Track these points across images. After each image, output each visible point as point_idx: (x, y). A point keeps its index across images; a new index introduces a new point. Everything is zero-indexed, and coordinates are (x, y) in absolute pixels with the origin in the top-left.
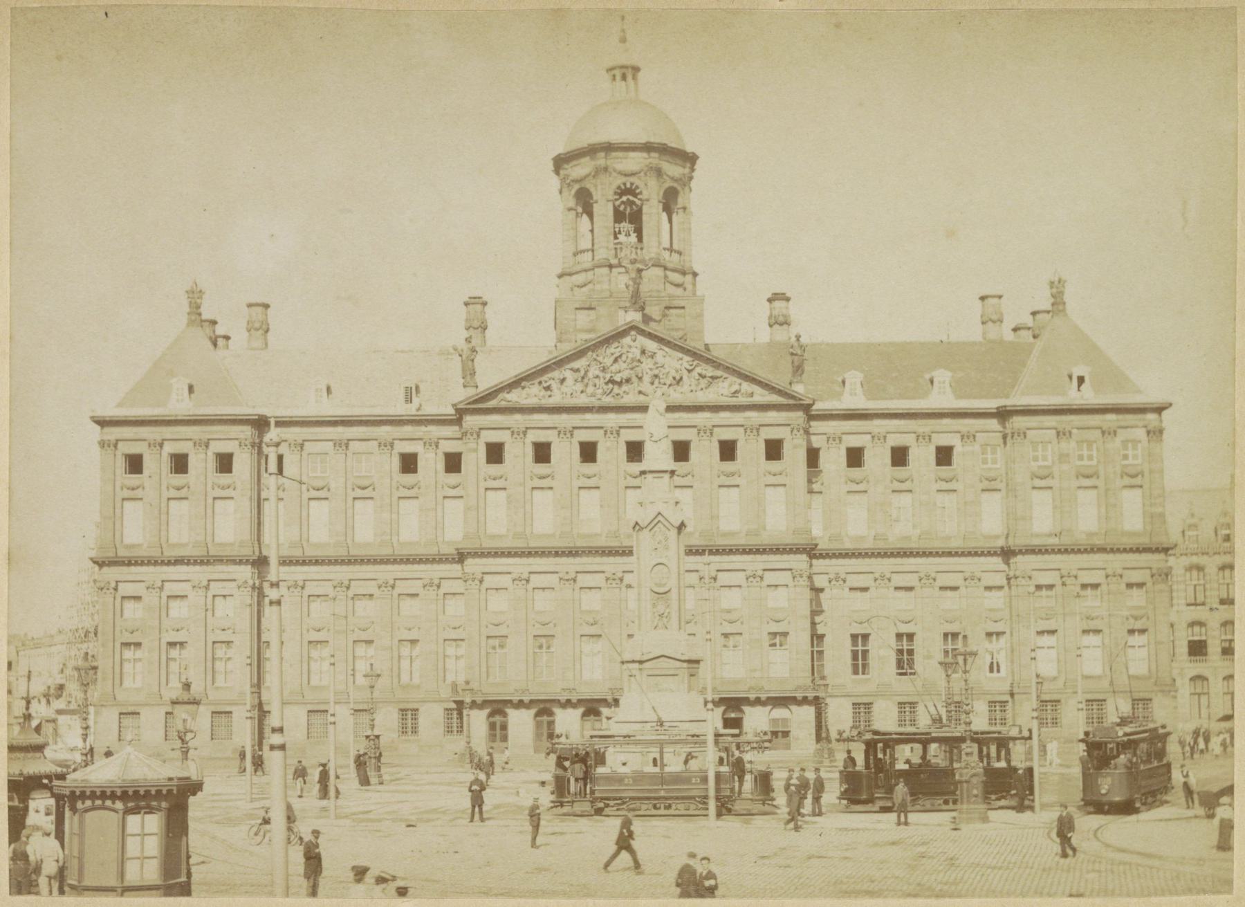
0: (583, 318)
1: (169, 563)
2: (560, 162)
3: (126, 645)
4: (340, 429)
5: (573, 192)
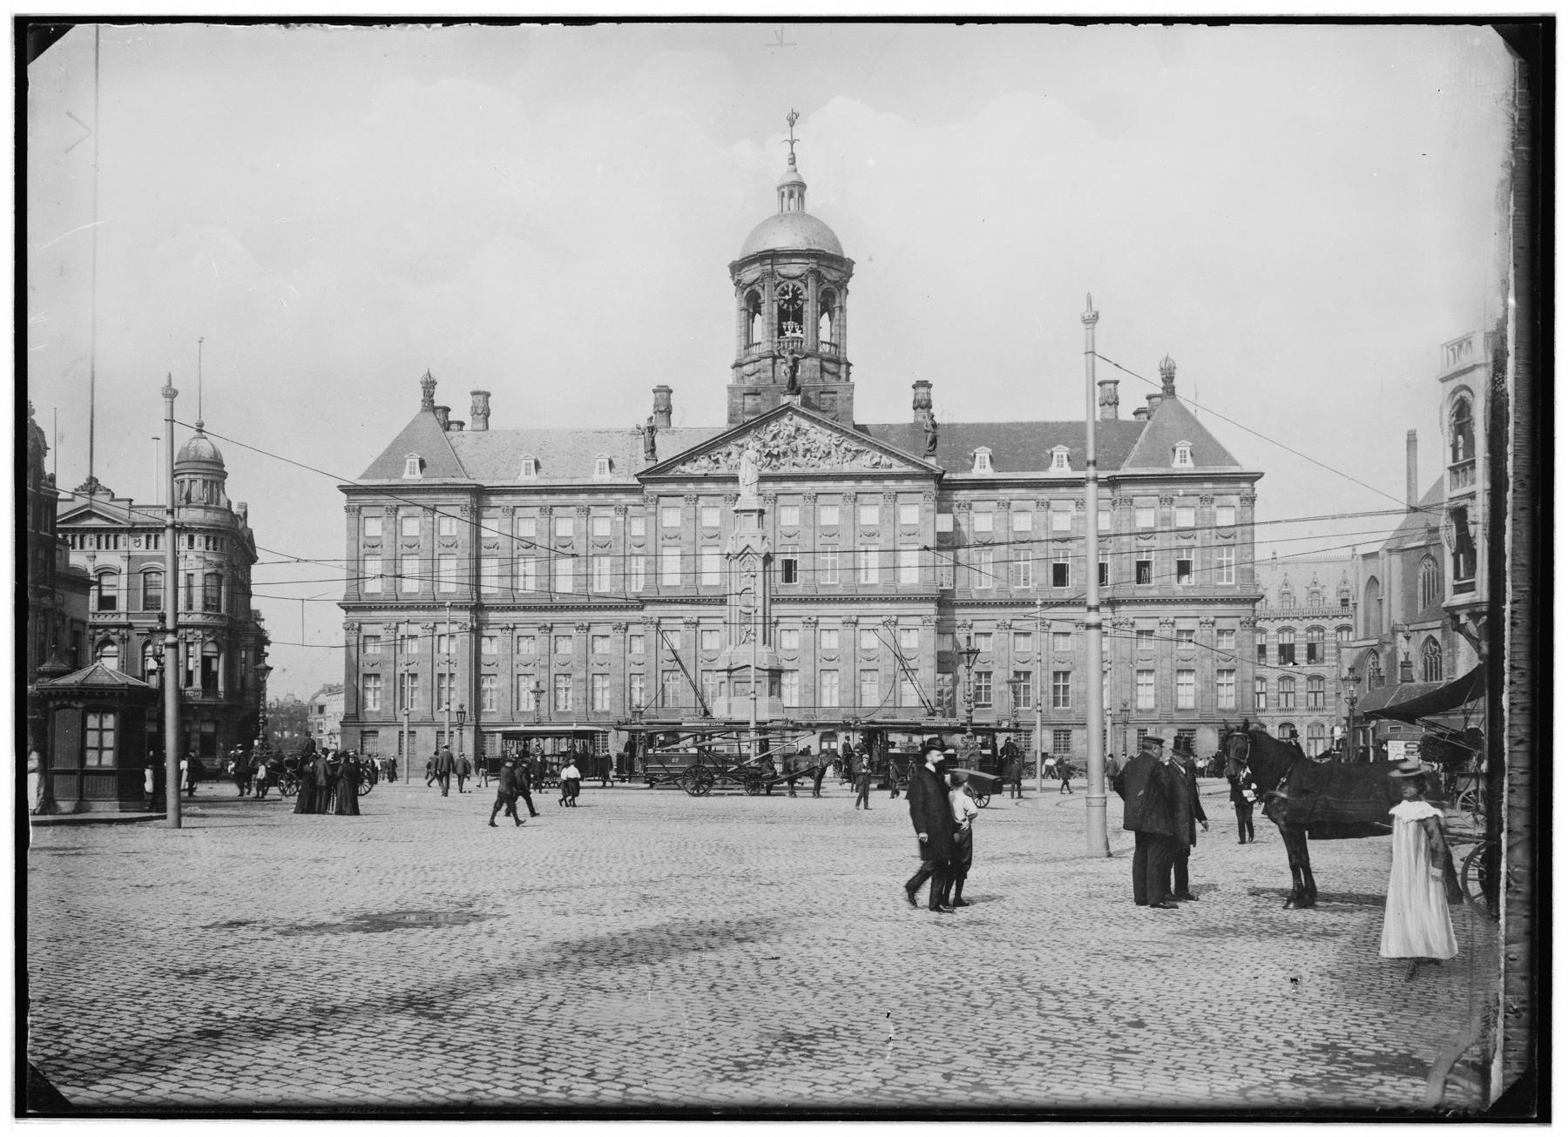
3: (367, 676)
4: (545, 497)
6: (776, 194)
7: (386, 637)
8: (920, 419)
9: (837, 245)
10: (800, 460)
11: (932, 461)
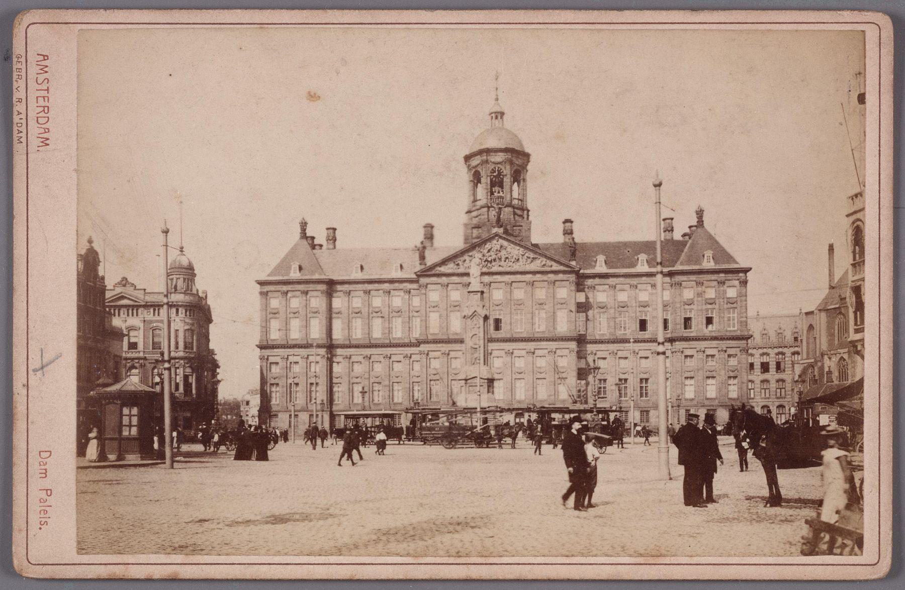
1: (290, 348)
2: (467, 158)
4: (366, 285)
7: (282, 364)
8: (567, 240)
9: (522, 145)
10: (502, 263)
11: (573, 263)
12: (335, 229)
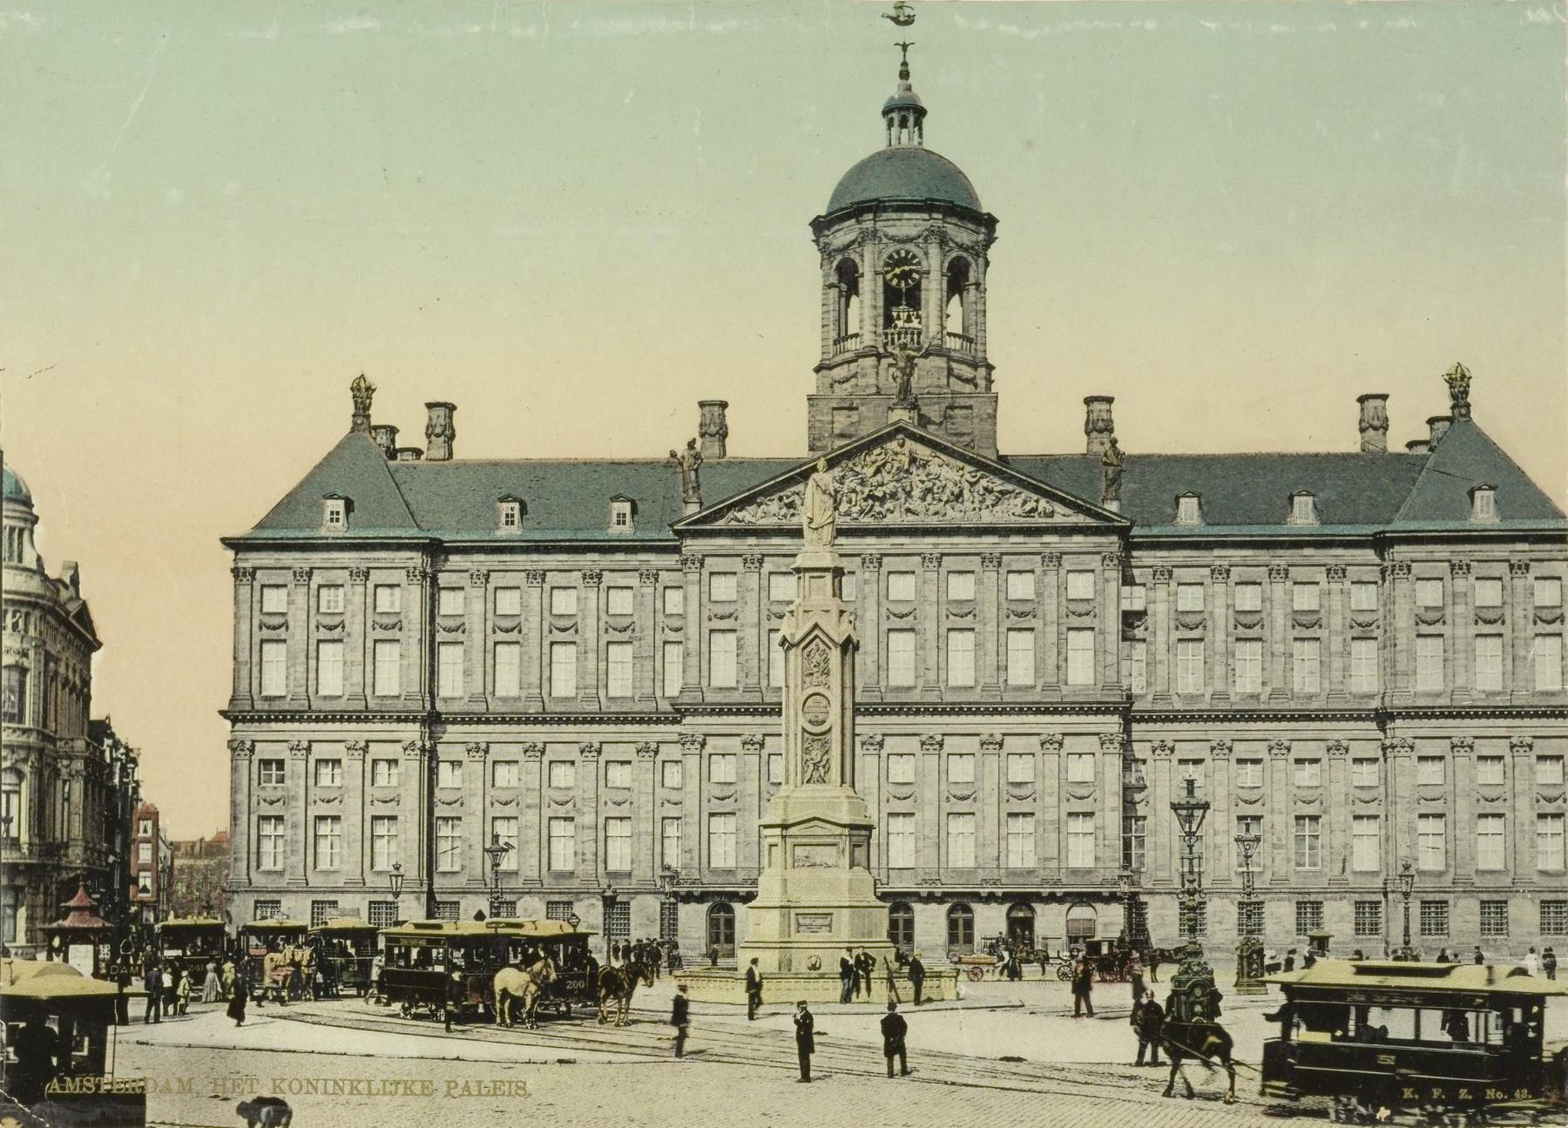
0: (842, 421)
5: (835, 263)
6: (884, 122)
8: (1096, 448)
9: (972, 197)
12: (451, 408)
